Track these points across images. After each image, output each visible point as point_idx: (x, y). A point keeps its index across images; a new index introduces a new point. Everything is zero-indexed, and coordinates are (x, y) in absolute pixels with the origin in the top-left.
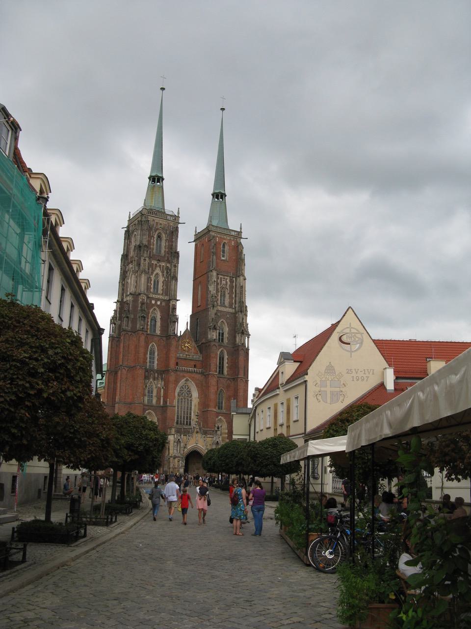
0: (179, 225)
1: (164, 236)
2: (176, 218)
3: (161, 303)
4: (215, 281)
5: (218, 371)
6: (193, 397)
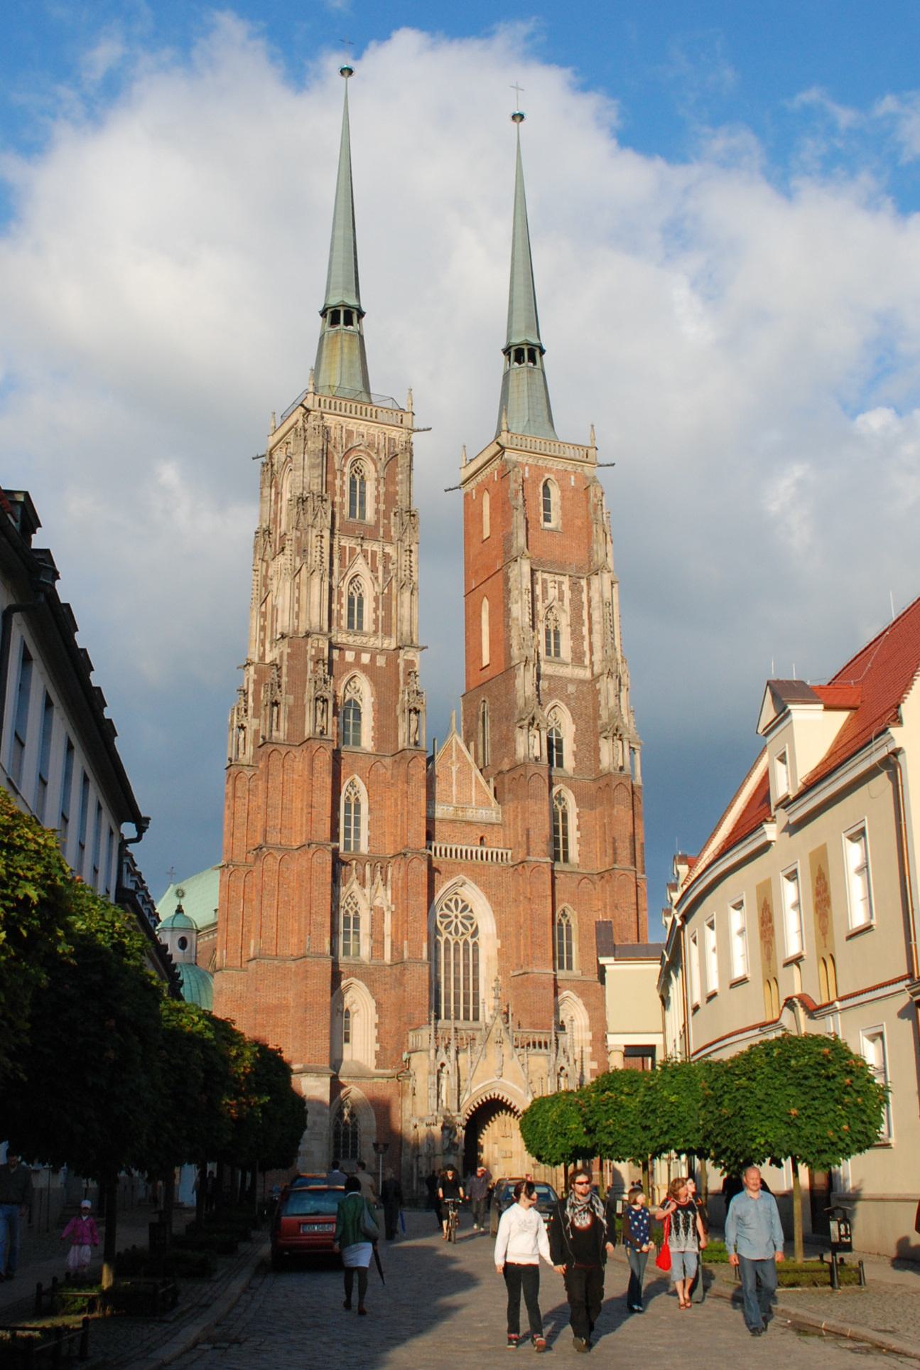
0: (415, 437)
1: (369, 470)
3: (373, 659)
6: (481, 934)
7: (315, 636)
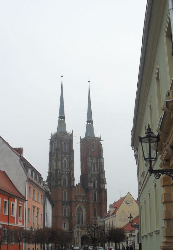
2: (71, 135)
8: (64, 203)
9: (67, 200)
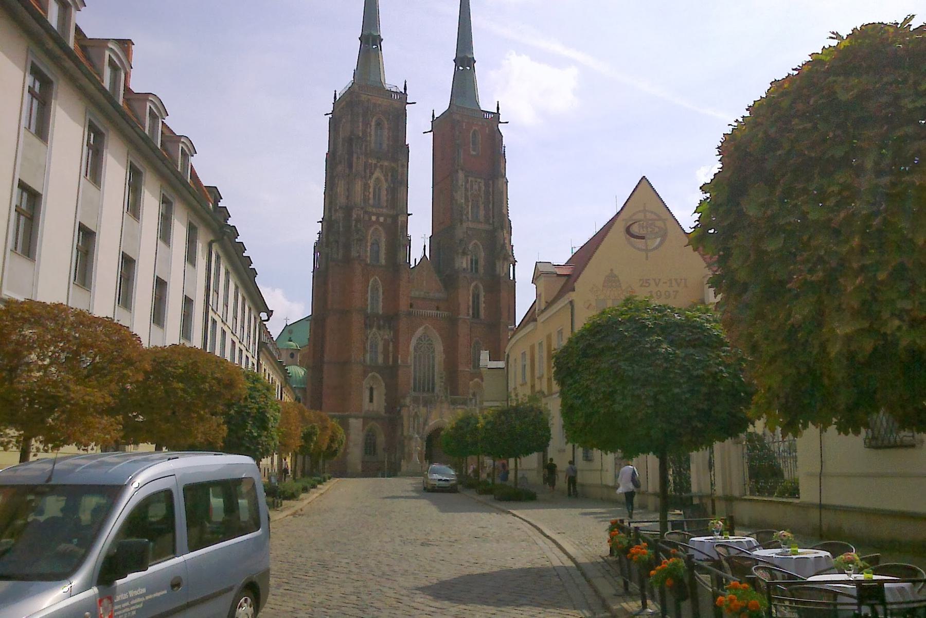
3: (385, 220)
4: (462, 185)
5: (471, 313)
7: (356, 209)
8: (369, 321)
9: (381, 312)
